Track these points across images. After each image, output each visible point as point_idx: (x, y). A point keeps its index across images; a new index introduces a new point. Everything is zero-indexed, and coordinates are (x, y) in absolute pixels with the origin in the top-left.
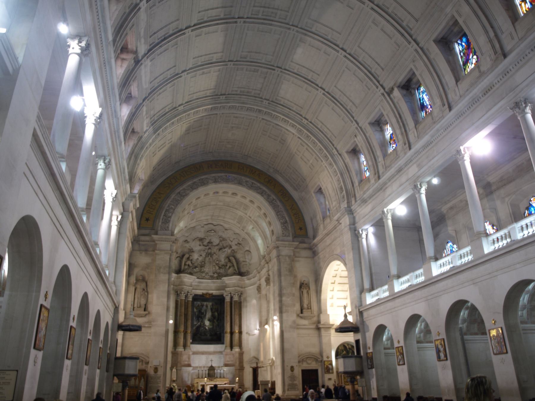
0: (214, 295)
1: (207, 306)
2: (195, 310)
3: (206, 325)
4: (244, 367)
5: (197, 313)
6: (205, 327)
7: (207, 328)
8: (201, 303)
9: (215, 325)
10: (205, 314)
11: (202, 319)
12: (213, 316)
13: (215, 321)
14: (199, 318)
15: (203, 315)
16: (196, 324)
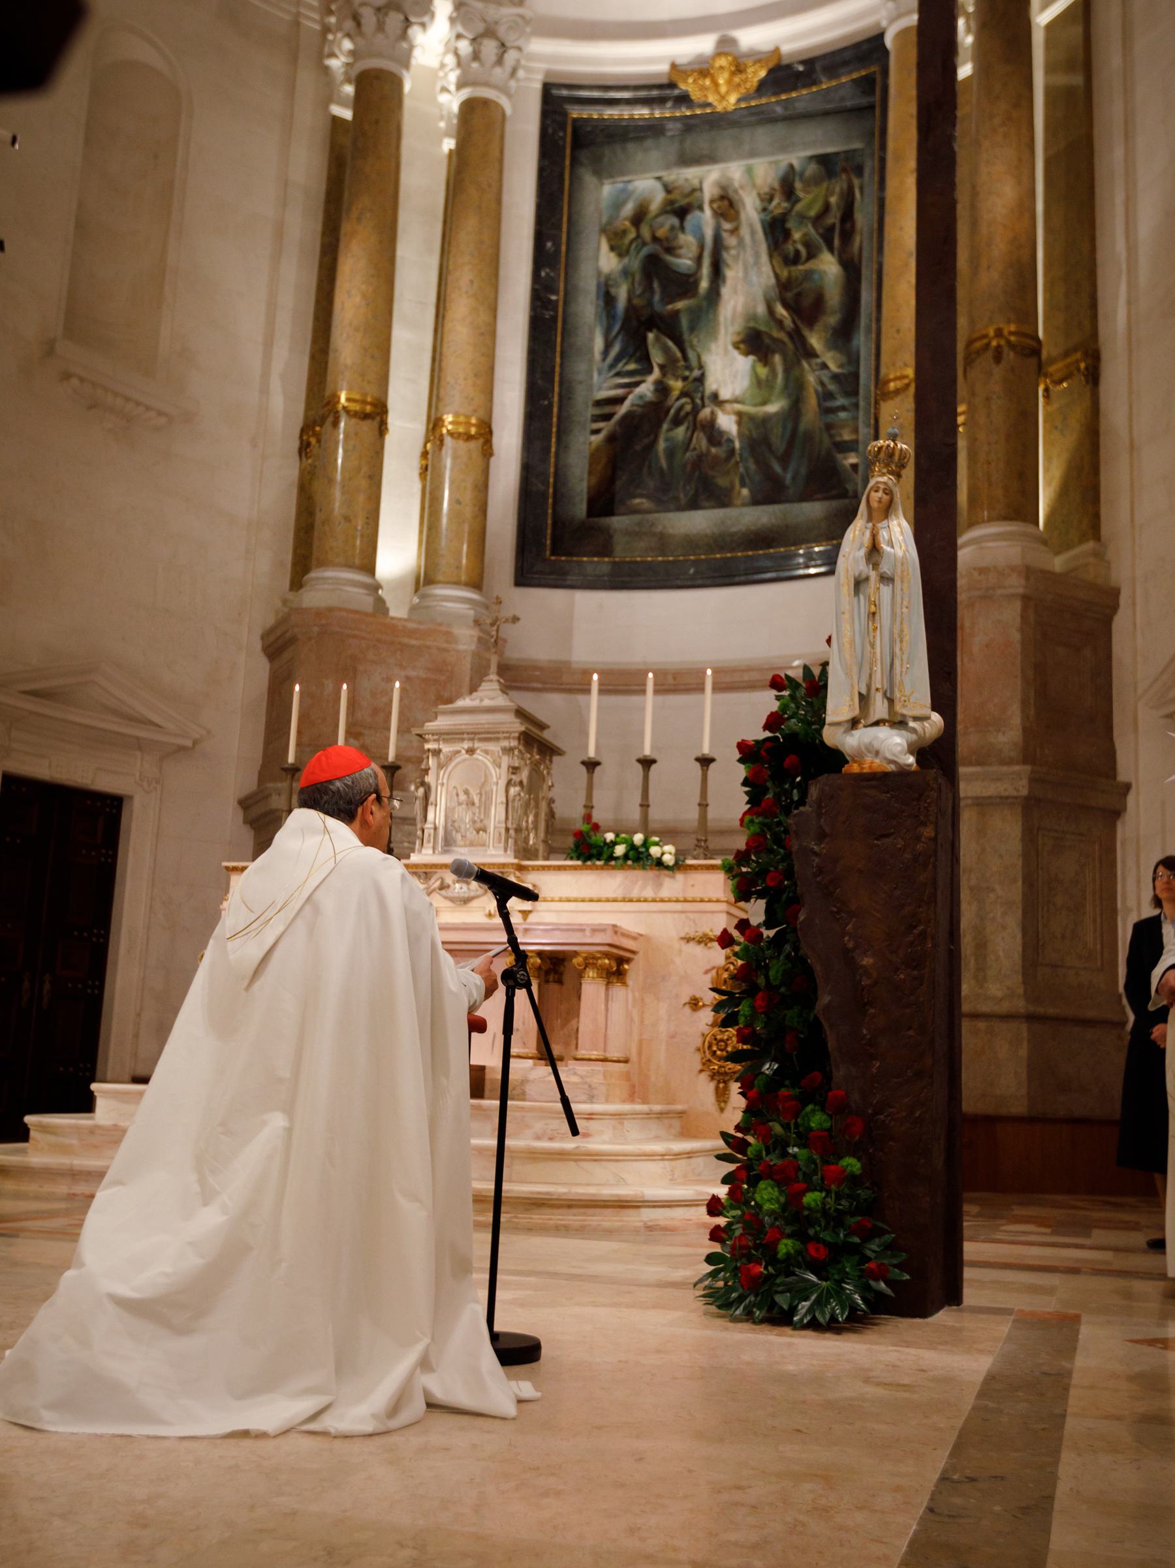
0: (789, 67)
1: (727, 205)
2: (608, 262)
3: (715, 396)
4: (1127, 787)
5: (622, 293)
6: (705, 413)
7: (727, 422)
8: (668, 189)
9: (811, 379)
10: (704, 284)
11: (680, 343)
12: (784, 286)
13: (815, 341)
14: (651, 336)
15: (680, 305)
16: (619, 400)
